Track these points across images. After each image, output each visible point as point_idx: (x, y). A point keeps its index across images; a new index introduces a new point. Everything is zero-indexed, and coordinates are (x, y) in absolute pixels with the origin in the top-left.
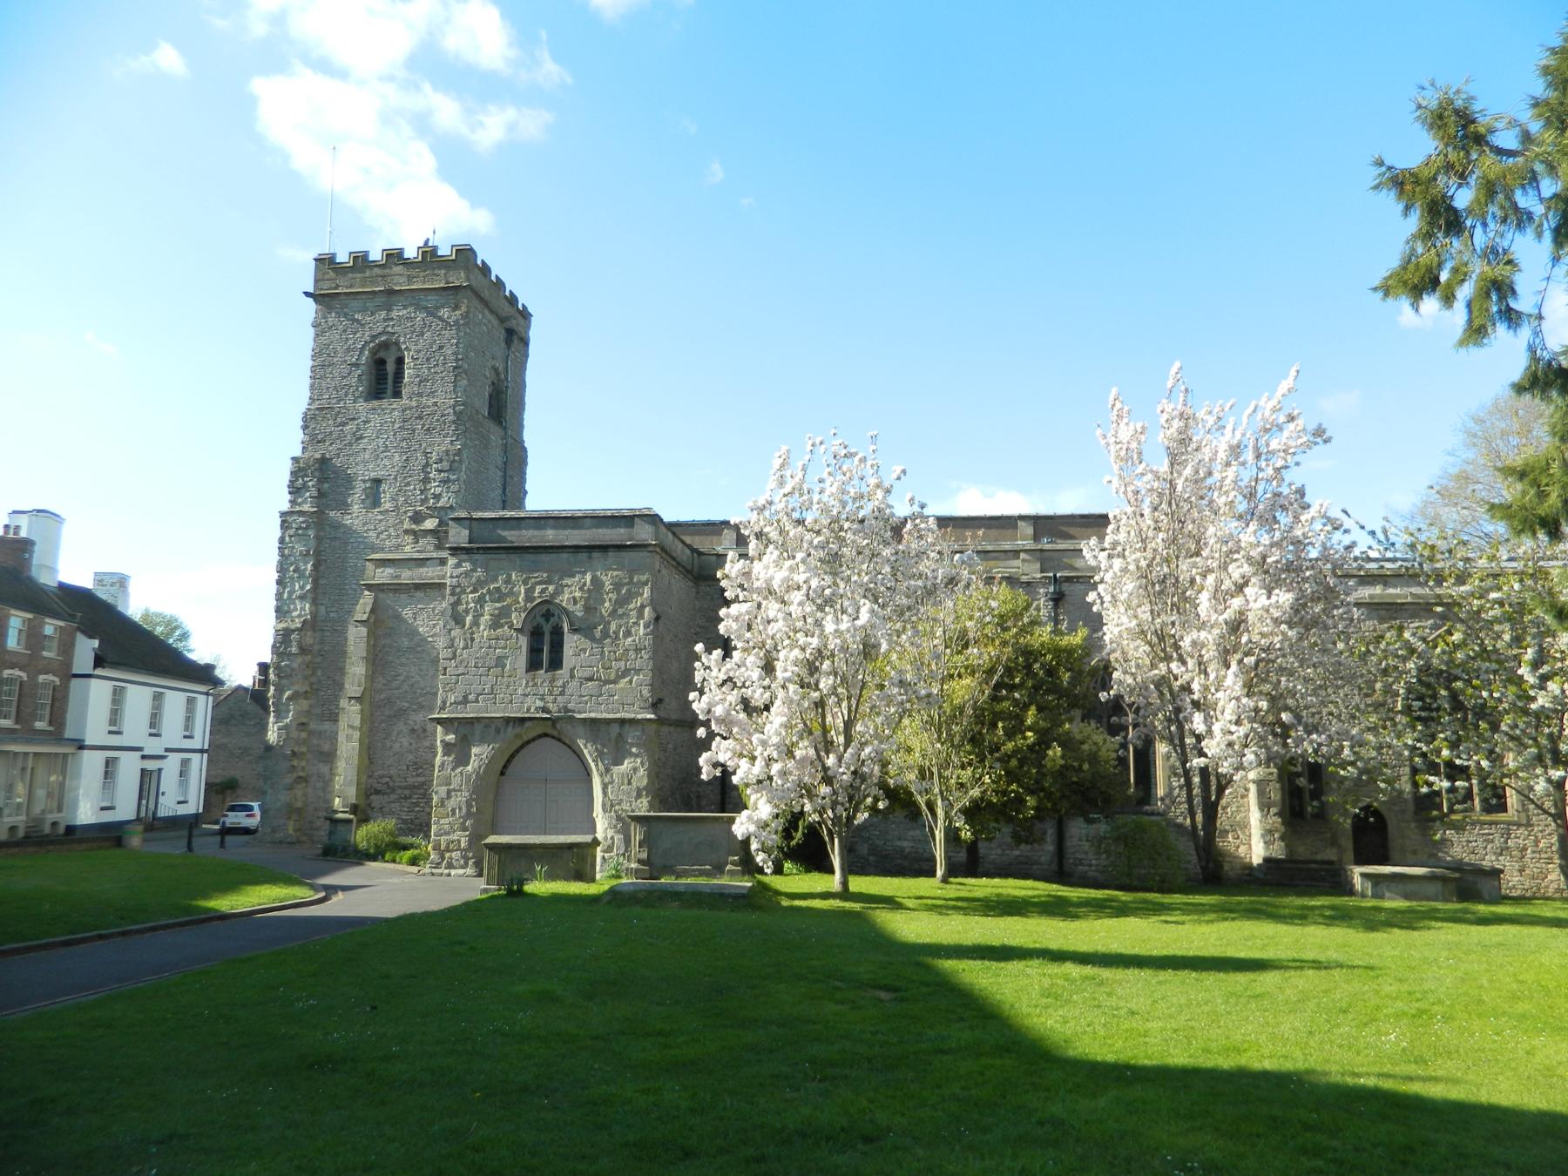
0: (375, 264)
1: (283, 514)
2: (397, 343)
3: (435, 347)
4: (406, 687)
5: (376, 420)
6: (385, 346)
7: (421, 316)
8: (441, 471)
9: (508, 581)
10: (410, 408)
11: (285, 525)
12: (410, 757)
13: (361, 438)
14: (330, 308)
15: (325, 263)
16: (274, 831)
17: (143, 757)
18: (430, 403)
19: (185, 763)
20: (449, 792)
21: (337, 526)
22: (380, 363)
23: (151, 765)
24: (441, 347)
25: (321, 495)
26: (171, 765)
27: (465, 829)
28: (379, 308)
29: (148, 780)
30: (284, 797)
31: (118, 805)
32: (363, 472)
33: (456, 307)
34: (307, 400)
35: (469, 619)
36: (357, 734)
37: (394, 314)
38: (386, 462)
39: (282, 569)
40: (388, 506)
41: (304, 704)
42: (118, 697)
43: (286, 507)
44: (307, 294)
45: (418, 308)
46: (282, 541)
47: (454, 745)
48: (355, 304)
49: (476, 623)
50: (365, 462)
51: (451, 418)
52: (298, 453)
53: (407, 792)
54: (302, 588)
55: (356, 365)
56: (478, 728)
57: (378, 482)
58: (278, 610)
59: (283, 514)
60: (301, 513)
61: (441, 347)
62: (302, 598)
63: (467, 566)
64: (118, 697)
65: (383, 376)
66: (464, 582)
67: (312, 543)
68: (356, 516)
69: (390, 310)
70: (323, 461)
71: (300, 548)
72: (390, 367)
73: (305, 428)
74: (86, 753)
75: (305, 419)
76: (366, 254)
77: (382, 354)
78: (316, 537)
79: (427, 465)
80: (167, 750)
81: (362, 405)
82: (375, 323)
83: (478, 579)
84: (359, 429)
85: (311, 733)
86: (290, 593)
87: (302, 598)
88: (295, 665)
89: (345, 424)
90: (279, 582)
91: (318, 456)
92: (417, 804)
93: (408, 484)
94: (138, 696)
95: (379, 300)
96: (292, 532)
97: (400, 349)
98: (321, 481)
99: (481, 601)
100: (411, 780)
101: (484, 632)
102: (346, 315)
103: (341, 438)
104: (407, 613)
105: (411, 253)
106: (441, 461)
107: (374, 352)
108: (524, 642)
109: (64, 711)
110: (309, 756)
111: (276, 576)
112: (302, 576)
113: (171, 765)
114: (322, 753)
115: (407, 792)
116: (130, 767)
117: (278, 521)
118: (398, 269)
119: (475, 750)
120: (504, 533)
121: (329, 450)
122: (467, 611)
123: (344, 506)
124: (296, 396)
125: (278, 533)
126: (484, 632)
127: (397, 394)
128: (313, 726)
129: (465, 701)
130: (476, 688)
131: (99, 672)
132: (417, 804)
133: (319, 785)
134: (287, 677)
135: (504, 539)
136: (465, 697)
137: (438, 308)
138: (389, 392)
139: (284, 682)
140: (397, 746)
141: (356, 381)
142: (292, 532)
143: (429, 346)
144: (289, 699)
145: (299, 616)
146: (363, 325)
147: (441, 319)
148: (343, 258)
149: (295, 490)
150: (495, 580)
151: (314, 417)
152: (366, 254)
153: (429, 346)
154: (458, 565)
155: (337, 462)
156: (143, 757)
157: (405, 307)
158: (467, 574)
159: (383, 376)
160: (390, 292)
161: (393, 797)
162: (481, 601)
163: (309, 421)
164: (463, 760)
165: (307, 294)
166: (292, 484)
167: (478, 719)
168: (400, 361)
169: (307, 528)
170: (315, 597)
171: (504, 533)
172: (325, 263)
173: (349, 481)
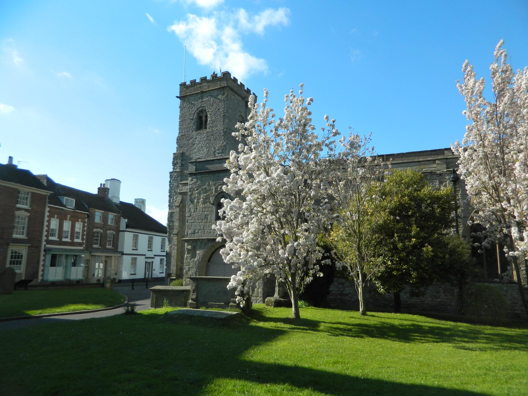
0: (199, 84)
1: (170, 173)
2: (205, 110)
3: (217, 109)
6: (202, 111)
8: (219, 153)
9: (209, 185)
10: (209, 132)
11: (171, 177)
13: (194, 144)
15: (183, 85)
17: (146, 258)
19: (161, 260)
20: (189, 268)
22: (200, 118)
23: (149, 260)
24: (219, 109)
25: (182, 165)
26: (157, 261)
28: (199, 98)
29: (149, 266)
31: (137, 273)
33: (224, 94)
34: (178, 133)
36: (176, 248)
37: (204, 100)
38: (202, 152)
39: (170, 192)
42: (136, 238)
43: (171, 170)
44: (177, 97)
45: (211, 96)
46: (170, 182)
47: (191, 250)
48: (192, 98)
49: (198, 202)
50: (196, 152)
51: (222, 134)
52: (175, 152)
55: (192, 119)
56: (199, 243)
58: (169, 206)
59: (170, 173)
60: (176, 172)
61: (219, 109)
63: (195, 180)
64: (136, 238)
65: (201, 122)
66: (194, 186)
69: (203, 99)
70: (183, 154)
72: (204, 119)
73: (177, 143)
74: (124, 256)
75: (177, 140)
76: (195, 80)
77: (201, 115)
79: (215, 152)
80: (155, 255)
81: (194, 133)
82: (198, 104)
83: (199, 185)
86: (173, 200)
89: (189, 140)
90: (170, 196)
91: (181, 152)
94: (143, 238)
95: (200, 95)
96: (173, 179)
97: (206, 112)
98: (182, 160)
99: (199, 193)
101: (201, 205)
105: (209, 78)
106: (219, 149)
107: (198, 114)
109: (117, 242)
111: (168, 194)
113: (157, 260)
116: (141, 261)
117: (169, 175)
118: (205, 84)
119: (198, 252)
120: (208, 166)
121: (184, 149)
122: (195, 198)
124: (175, 133)
125: (169, 179)
126: (201, 205)
127: (206, 128)
129: (194, 233)
130: (198, 227)
131: (127, 230)
135: (207, 169)
136: (194, 231)
137: (218, 95)
138: (203, 127)
141: (192, 125)
142: (173, 179)
143: (214, 109)
146: (194, 105)
147: (219, 99)
148: (188, 83)
149: (174, 164)
150: (205, 185)
152: (195, 80)
153: (214, 109)
154: (192, 180)
155: (187, 154)
156: (146, 258)
157: (207, 97)
158: (195, 183)
159: (201, 122)
160: (202, 92)
162: (199, 193)
163: (179, 140)
164: (194, 256)
165: (177, 97)
167: (199, 240)
168: (206, 116)
171: (208, 166)
172: (183, 85)
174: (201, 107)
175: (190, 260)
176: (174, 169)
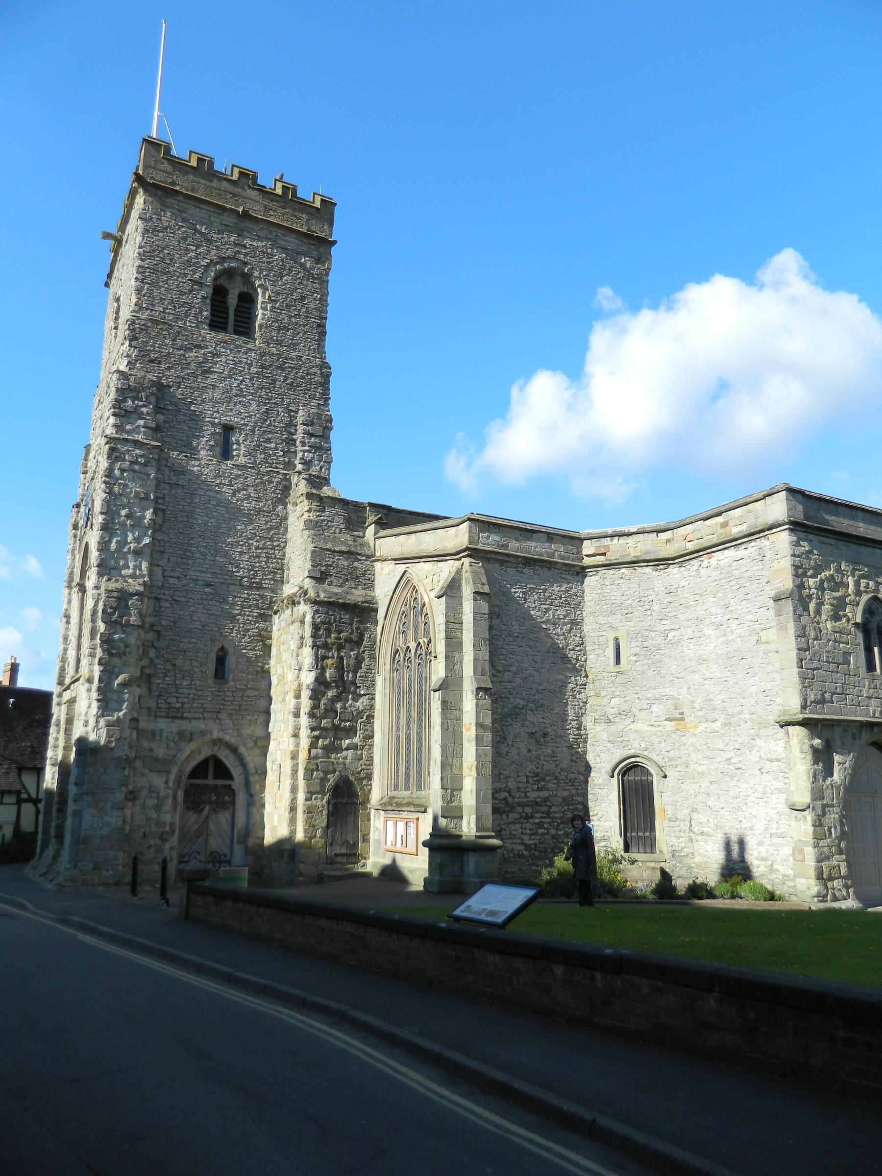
4: (518, 681)
5: (227, 357)
6: (229, 273)
7: (279, 256)
8: (311, 435)
10: (271, 355)
12: (531, 767)
13: (209, 371)
14: (165, 206)
16: (96, 868)
18: (294, 354)
20: (824, 806)
21: (182, 471)
22: (219, 293)
24: (303, 298)
27: (841, 852)
30: (114, 819)
32: (214, 415)
35: (812, 606)
36: (488, 736)
40: (242, 460)
41: (137, 691)
49: (818, 612)
50: (215, 402)
53: (528, 810)
54: (138, 540)
57: (228, 429)
61: (303, 298)
62: (137, 553)
65: (230, 310)
67: (152, 484)
68: (203, 463)
71: (135, 488)
72: (232, 301)
78: (156, 478)
84: (206, 361)
85: (141, 733)
87: (137, 553)
88: (132, 640)
91: (151, 377)
92: (540, 825)
93: (268, 441)
98: (158, 409)
100: (533, 795)
102: (184, 220)
103: (183, 363)
104: (517, 592)
105: (266, 180)
108: (860, 638)
110: (138, 764)
112: (137, 524)
114: (157, 760)
115: (528, 810)
119: (837, 758)
120: (827, 517)
123: (192, 452)
128: (142, 724)
129: (822, 701)
132: (540, 825)
133: (151, 802)
134: (119, 655)
135: (826, 522)
139: (116, 661)
140: (514, 752)
144: (124, 685)
145: (133, 576)
149: (122, 413)
151: (144, 329)
157: (260, 239)
160: (246, 215)
161: (513, 816)
162: (821, 588)
166: (118, 404)
168: (247, 300)
169: (145, 465)
170: (155, 553)
171: (827, 517)
173: (196, 419)
174: (234, 258)
175: (824, 780)
176: (119, 427)
